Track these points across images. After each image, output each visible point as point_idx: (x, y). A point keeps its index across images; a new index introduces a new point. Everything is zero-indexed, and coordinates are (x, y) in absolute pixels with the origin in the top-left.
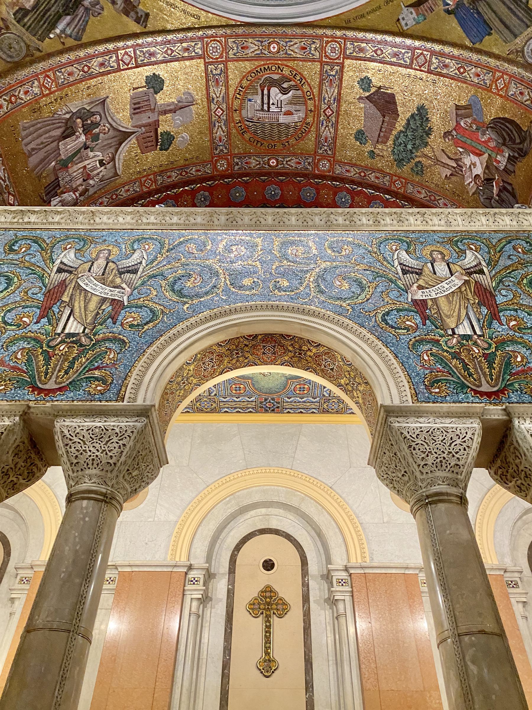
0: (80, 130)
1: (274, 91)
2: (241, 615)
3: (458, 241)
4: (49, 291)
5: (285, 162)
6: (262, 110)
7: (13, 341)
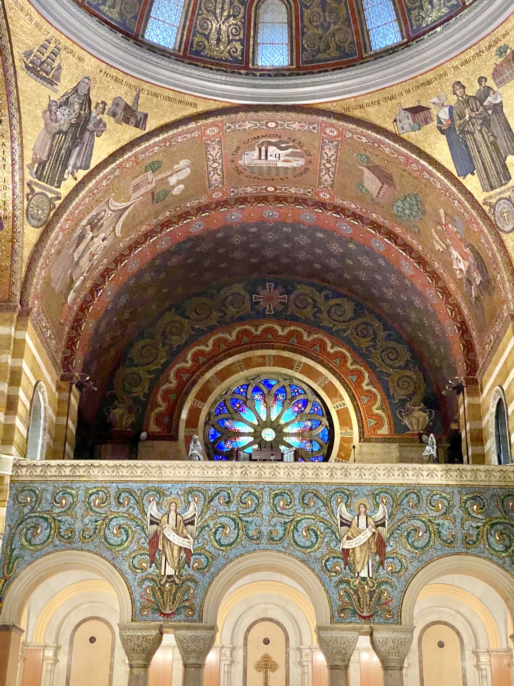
2: (251, 671)
3: (377, 493)
5: (285, 125)
7: (143, 581)
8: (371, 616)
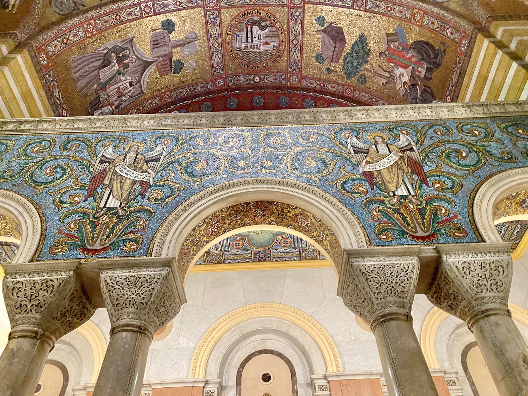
0: (115, 61)
1: (255, 28)
3: (394, 128)
4: (94, 177)
5: (265, 79)
6: (247, 42)
7: (68, 215)
8: (433, 235)
